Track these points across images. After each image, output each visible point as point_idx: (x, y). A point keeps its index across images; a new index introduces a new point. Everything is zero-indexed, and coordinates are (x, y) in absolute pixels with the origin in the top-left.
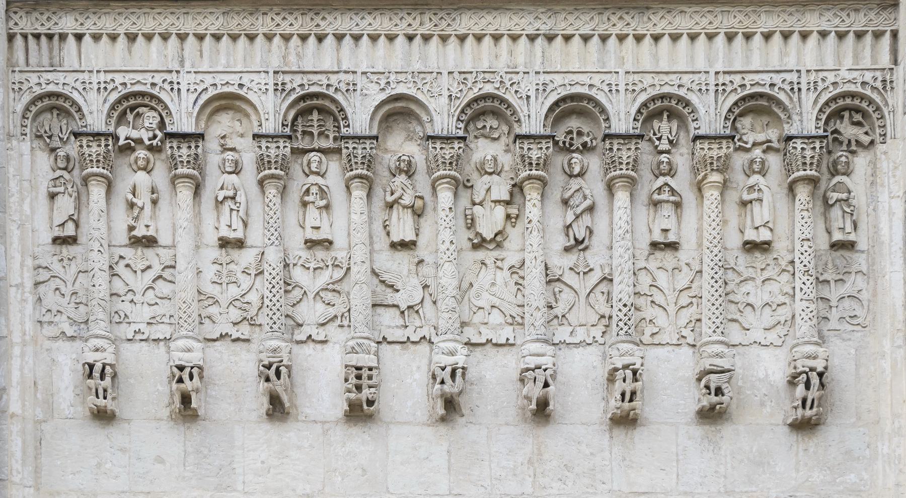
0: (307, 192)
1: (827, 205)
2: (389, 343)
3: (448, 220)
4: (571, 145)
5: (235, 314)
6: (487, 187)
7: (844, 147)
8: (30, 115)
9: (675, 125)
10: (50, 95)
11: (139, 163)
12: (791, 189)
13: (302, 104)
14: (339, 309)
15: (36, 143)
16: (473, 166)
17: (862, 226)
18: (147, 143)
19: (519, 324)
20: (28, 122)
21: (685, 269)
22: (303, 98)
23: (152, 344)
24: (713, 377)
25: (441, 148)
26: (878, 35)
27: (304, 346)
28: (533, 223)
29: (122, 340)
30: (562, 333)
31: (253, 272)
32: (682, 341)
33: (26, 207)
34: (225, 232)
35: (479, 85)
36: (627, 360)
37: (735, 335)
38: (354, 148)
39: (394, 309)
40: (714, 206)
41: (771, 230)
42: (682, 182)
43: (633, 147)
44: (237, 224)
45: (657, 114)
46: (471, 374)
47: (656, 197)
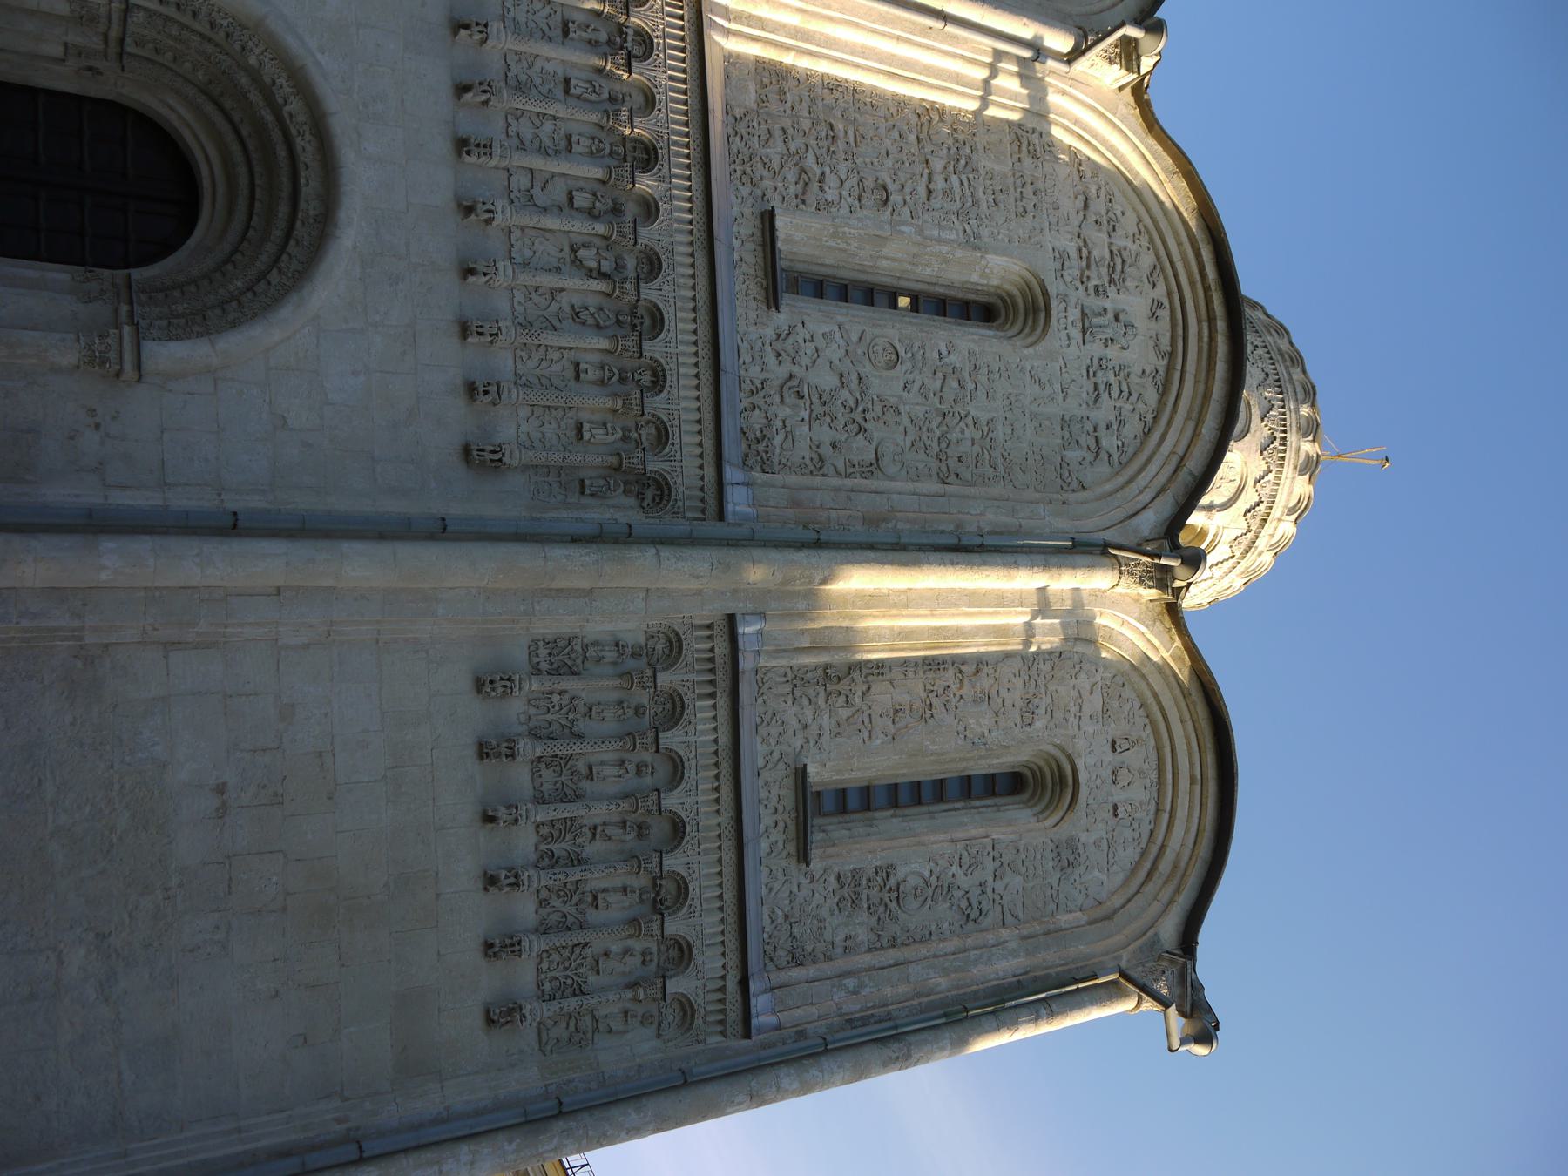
5: (523, 78)
26: (703, 511)
34: (573, 82)
44: (578, 91)
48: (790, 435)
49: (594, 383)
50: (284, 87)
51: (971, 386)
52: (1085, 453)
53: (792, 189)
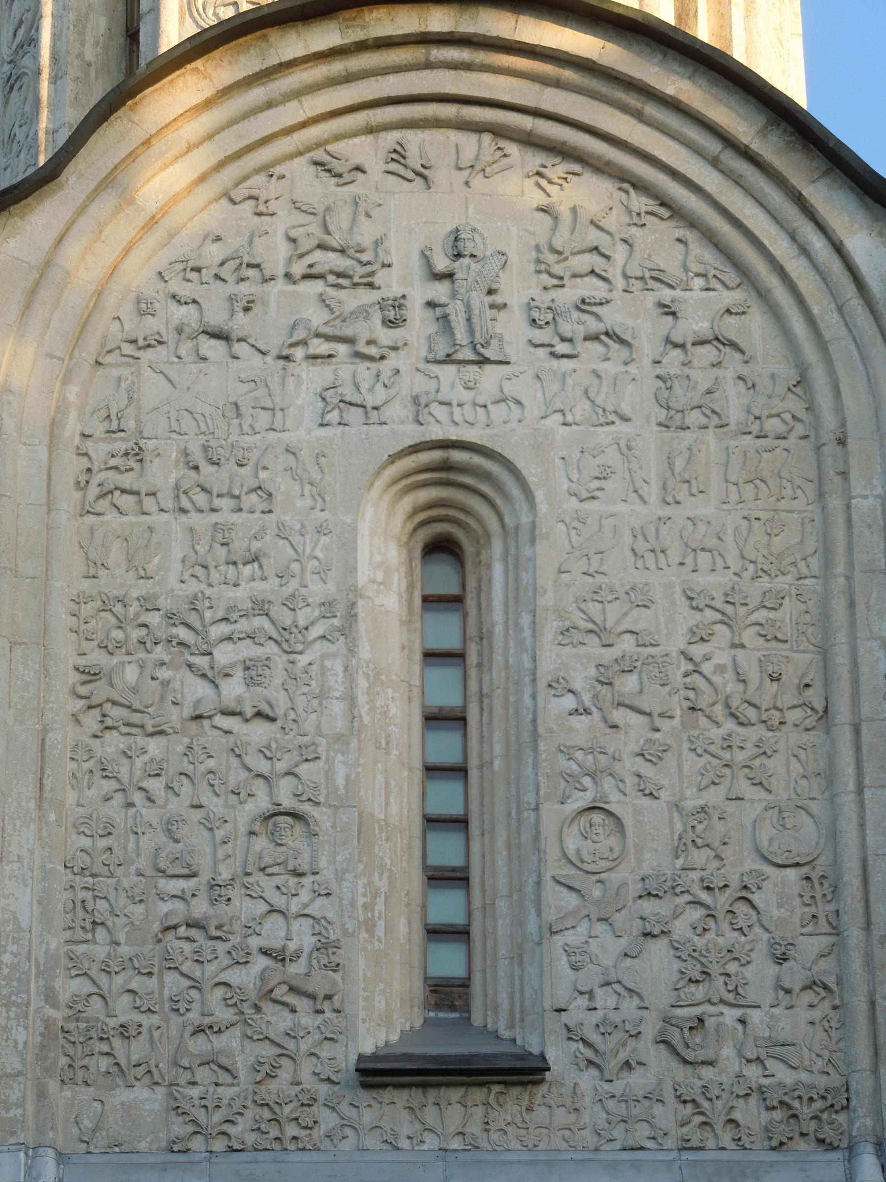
48: (779, 1047)
51: (627, 644)
52: (728, 374)
53: (307, 1020)
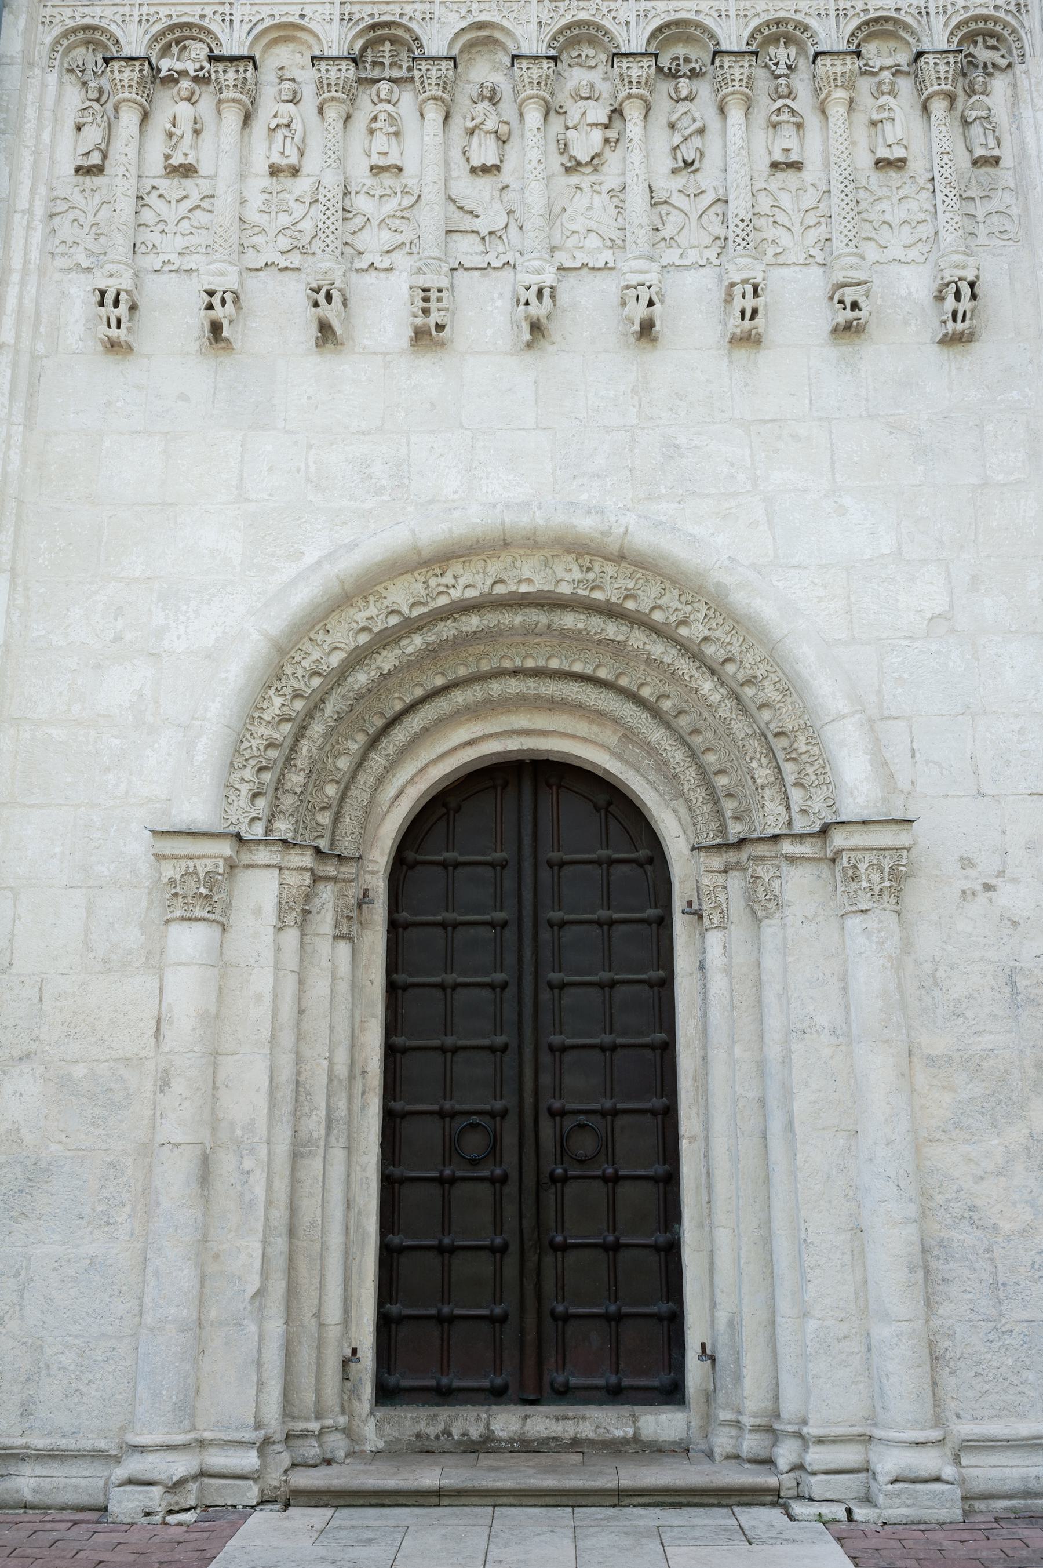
0: (375, 119)
1: (966, 123)
2: (466, 269)
3: (535, 140)
4: (678, 71)
5: (284, 243)
6: (583, 110)
7: (980, 69)
8: (61, 49)
9: (792, 51)
10: (86, 28)
11: (182, 93)
12: (925, 108)
13: (372, 34)
14: (407, 236)
15: (67, 77)
16: (567, 93)
17: (1006, 143)
18: (192, 74)
19: (620, 247)
20: (58, 56)
21: (811, 189)
22: (373, 27)
23: (184, 275)
24: (847, 290)
25: (528, 69)
27: (366, 275)
28: (633, 143)
29: (148, 271)
30: (671, 256)
31: (308, 200)
32: (811, 260)
33: (46, 136)
34: (276, 159)
35: (572, 13)
36: (745, 275)
37: (871, 252)
38: (428, 70)
39: (474, 235)
40: (840, 122)
41: (906, 148)
42: (804, 102)
43: (746, 65)
45: (773, 40)
46: (563, 298)
47: (774, 118)
49: (802, 140)
50: (369, 614)
